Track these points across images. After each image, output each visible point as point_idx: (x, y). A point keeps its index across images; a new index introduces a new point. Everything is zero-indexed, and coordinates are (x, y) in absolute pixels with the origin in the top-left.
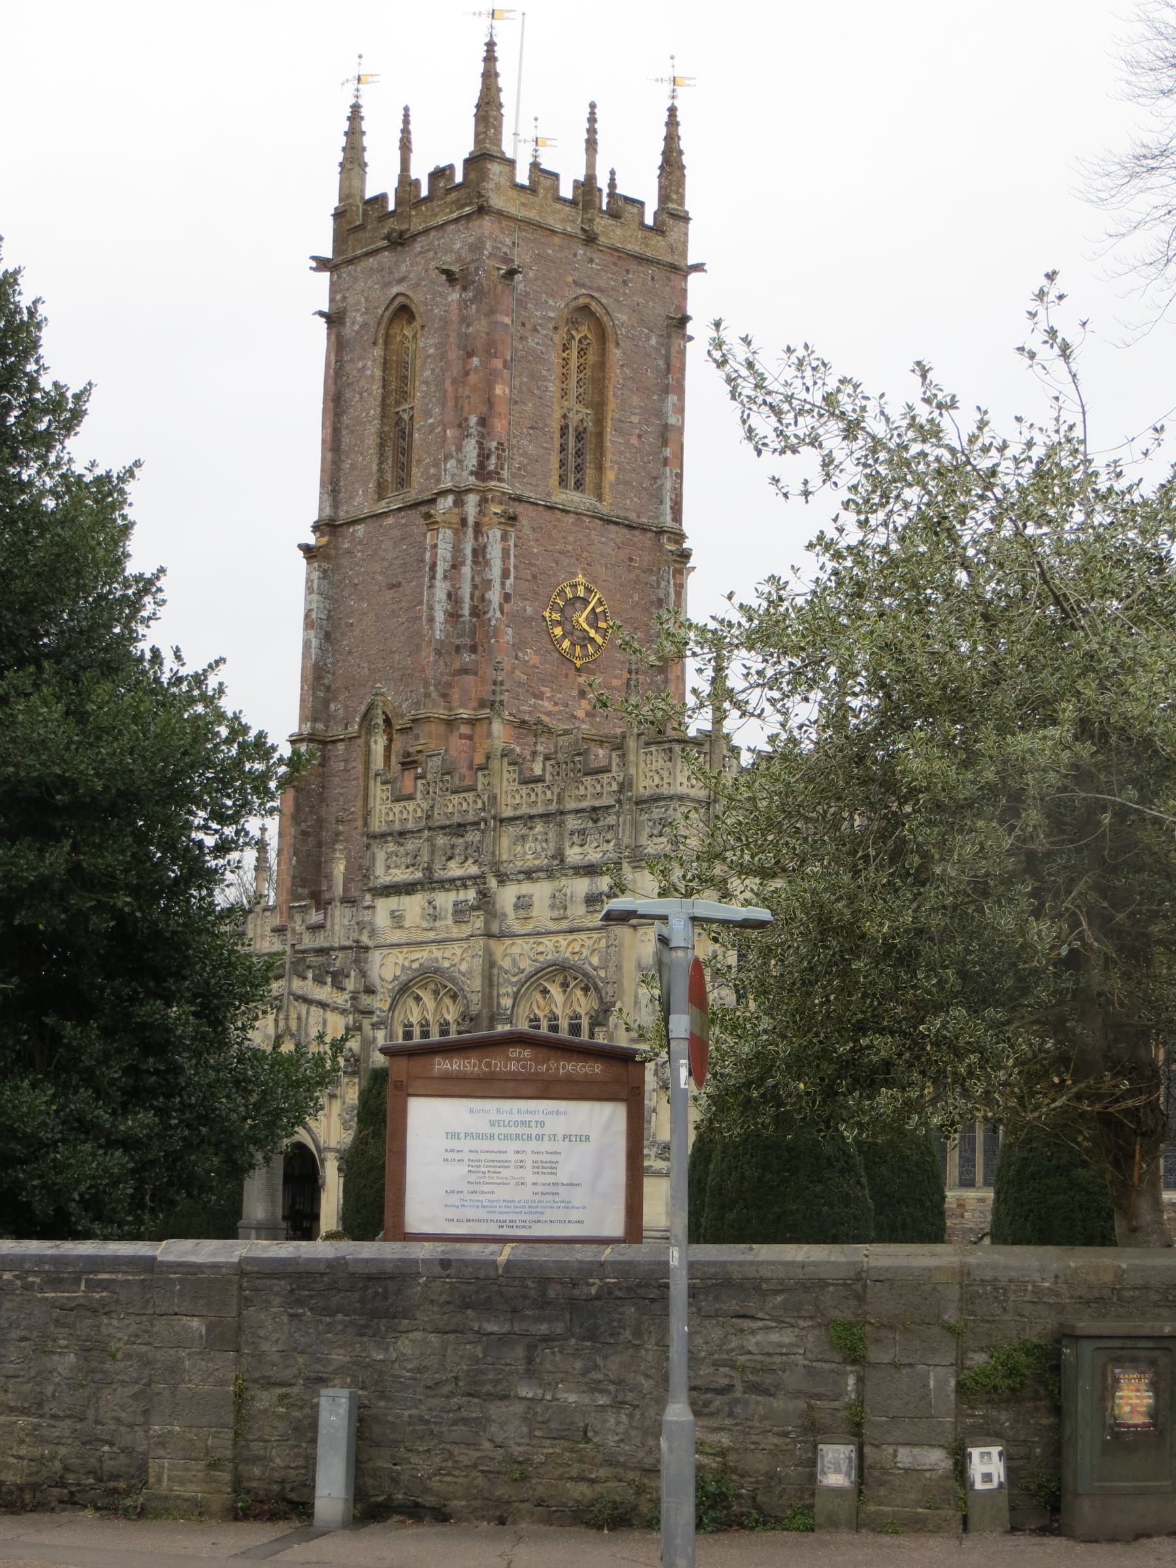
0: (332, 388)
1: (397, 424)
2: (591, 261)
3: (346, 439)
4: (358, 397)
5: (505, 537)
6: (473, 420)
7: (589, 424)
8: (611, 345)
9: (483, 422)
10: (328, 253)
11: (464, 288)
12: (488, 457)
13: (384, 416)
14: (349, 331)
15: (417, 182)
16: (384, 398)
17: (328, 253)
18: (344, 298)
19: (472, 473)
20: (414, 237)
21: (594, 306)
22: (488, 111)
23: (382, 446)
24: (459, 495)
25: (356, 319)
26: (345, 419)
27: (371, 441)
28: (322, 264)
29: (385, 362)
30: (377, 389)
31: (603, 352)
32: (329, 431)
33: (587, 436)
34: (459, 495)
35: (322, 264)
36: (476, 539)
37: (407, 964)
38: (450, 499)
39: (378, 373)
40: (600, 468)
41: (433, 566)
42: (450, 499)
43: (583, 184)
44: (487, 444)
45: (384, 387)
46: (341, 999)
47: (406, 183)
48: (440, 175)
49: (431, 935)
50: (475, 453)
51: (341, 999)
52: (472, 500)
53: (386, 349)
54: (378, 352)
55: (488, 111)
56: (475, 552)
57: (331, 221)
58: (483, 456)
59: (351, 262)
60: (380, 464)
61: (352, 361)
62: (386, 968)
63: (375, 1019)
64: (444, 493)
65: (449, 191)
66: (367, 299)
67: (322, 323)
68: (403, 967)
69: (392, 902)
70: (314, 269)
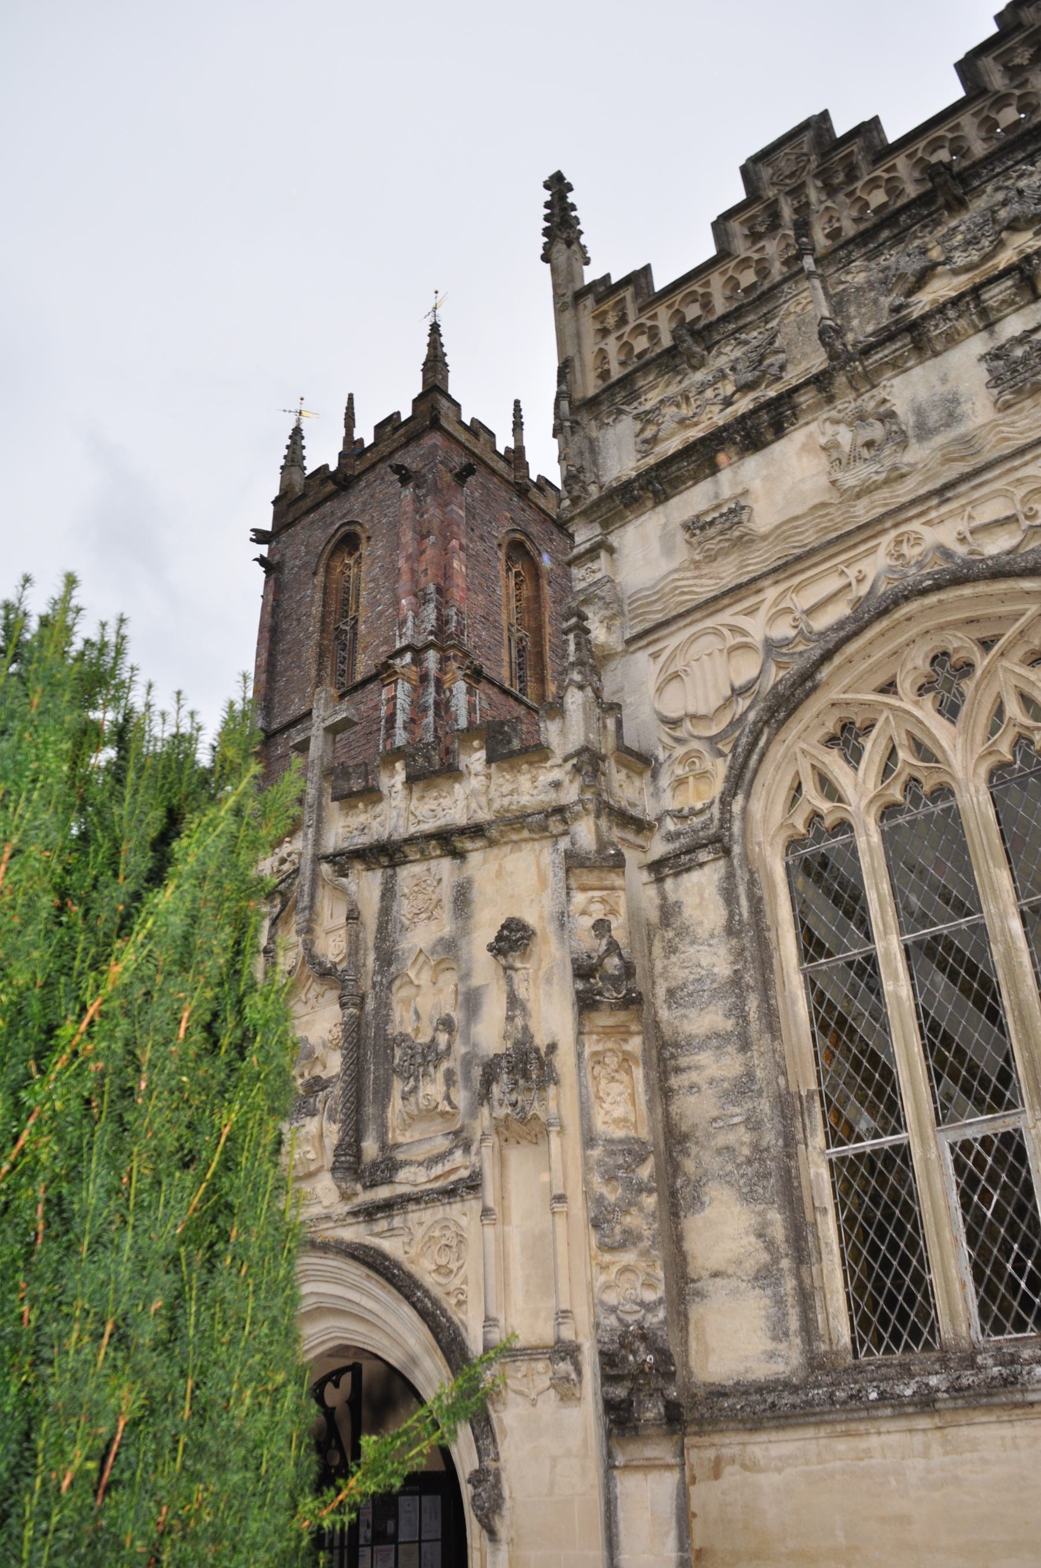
0: (269, 621)
1: (337, 638)
2: (523, 510)
3: (282, 662)
4: (295, 623)
5: (470, 691)
6: (432, 588)
7: (528, 643)
8: (544, 582)
9: (439, 590)
10: (267, 526)
11: (418, 486)
12: (447, 622)
13: (322, 631)
14: (287, 576)
15: (361, 441)
16: (323, 617)
17: (267, 526)
18: (283, 555)
19: (431, 633)
20: (359, 477)
21: (528, 544)
22: (435, 365)
23: (321, 655)
24: (418, 652)
25: (293, 565)
26: (281, 646)
27: (310, 653)
28: (260, 536)
29: (325, 588)
30: (316, 610)
31: (538, 588)
32: (265, 656)
33: (526, 654)
34: (418, 652)
35: (260, 536)
36: (438, 692)
37: (783, 630)
38: (408, 657)
39: (318, 596)
40: (542, 680)
41: (391, 719)
42: (408, 657)
43: (514, 451)
44: (444, 612)
45: (324, 606)
46: (530, 788)
47: (352, 448)
48: (388, 426)
49: (905, 492)
50: (433, 616)
51: (530, 788)
52: (432, 658)
53: (326, 577)
54: (319, 579)
55: (435, 365)
56: (437, 704)
57: (271, 508)
58: (442, 621)
59: (289, 525)
60: (319, 670)
61: (291, 597)
62: (686, 684)
63: (659, 848)
64: (400, 653)
65: (395, 430)
66: (306, 546)
67: (260, 572)
68: (771, 647)
69: (695, 499)
70: (252, 540)
